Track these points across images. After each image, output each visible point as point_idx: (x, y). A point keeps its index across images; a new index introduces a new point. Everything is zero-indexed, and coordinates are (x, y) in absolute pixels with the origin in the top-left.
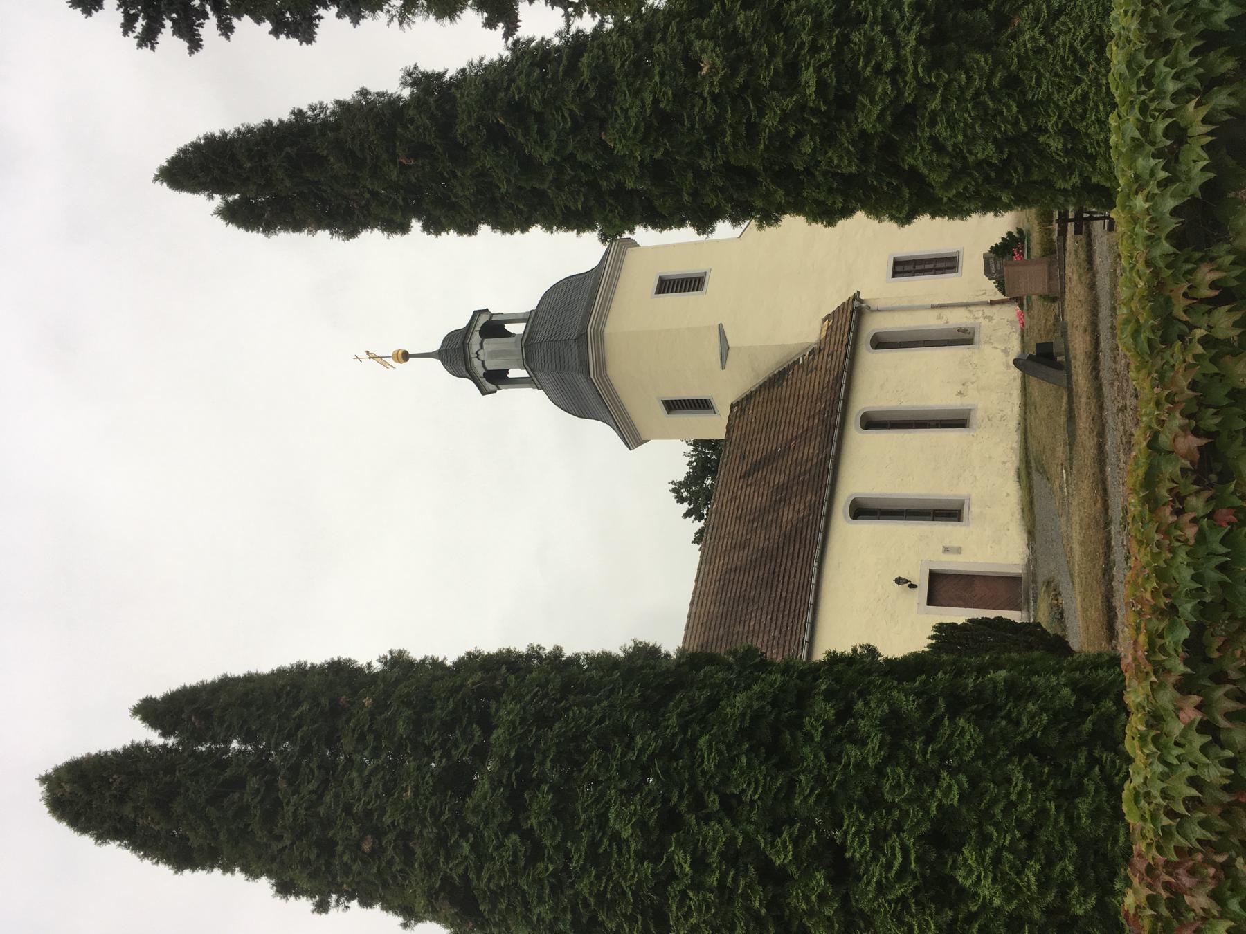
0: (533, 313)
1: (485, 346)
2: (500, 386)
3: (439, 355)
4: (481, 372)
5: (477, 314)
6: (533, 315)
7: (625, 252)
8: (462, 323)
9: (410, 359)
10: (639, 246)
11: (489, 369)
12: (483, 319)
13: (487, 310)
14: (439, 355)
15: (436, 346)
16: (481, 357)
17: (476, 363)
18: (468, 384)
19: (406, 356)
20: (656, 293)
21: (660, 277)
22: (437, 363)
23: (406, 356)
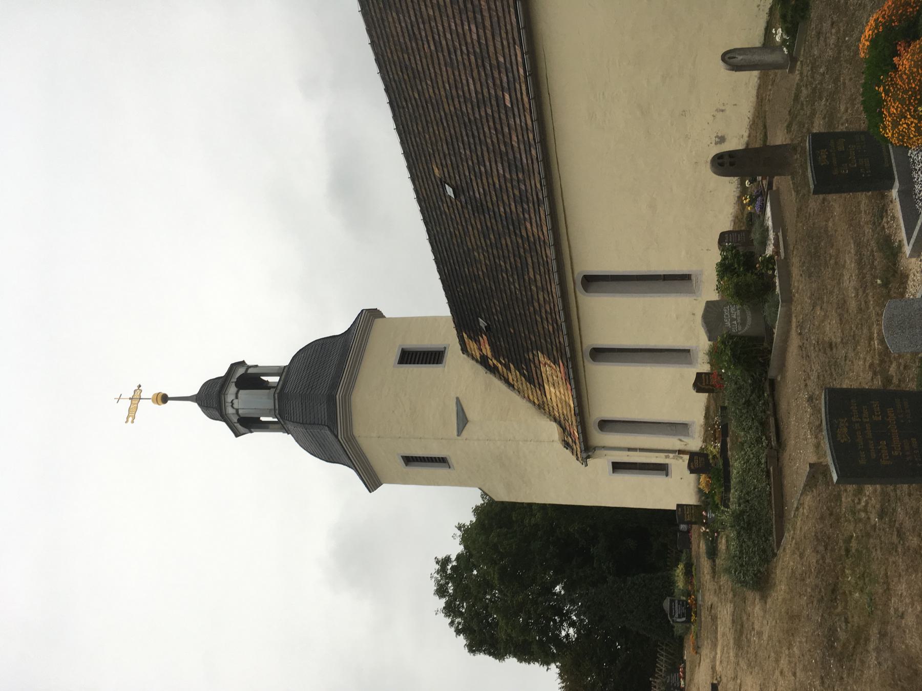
0: (286, 368)
1: (239, 395)
2: (252, 430)
3: (196, 399)
4: (235, 419)
5: (234, 367)
6: (285, 370)
7: (373, 321)
8: (222, 372)
9: (169, 402)
10: (384, 317)
11: (242, 416)
12: (241, 371)
13: (243, 362)
14: (196, 399)
15: (195, 391)
16: (236, 406)
17: (230, 411)
18: (222, 425)
19: (165, 399)
20: (398, 364)
21: (402, 349)
22: (194, 407)
23: (165, 399)
